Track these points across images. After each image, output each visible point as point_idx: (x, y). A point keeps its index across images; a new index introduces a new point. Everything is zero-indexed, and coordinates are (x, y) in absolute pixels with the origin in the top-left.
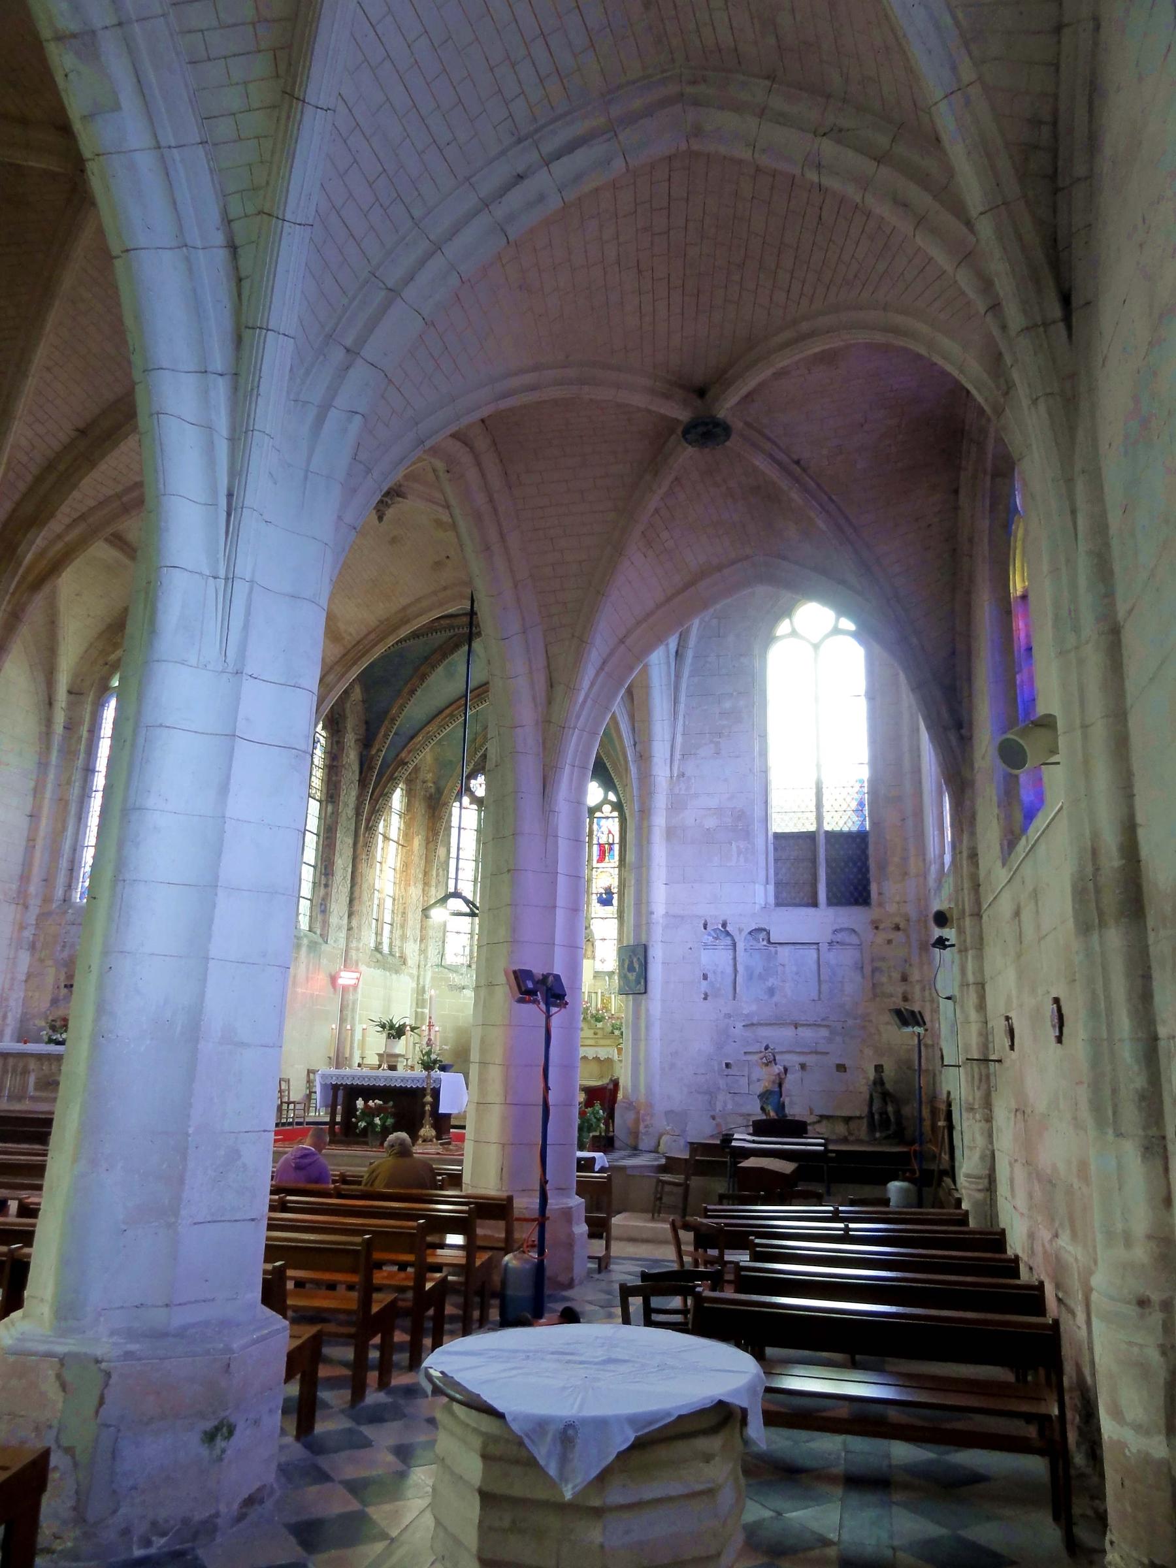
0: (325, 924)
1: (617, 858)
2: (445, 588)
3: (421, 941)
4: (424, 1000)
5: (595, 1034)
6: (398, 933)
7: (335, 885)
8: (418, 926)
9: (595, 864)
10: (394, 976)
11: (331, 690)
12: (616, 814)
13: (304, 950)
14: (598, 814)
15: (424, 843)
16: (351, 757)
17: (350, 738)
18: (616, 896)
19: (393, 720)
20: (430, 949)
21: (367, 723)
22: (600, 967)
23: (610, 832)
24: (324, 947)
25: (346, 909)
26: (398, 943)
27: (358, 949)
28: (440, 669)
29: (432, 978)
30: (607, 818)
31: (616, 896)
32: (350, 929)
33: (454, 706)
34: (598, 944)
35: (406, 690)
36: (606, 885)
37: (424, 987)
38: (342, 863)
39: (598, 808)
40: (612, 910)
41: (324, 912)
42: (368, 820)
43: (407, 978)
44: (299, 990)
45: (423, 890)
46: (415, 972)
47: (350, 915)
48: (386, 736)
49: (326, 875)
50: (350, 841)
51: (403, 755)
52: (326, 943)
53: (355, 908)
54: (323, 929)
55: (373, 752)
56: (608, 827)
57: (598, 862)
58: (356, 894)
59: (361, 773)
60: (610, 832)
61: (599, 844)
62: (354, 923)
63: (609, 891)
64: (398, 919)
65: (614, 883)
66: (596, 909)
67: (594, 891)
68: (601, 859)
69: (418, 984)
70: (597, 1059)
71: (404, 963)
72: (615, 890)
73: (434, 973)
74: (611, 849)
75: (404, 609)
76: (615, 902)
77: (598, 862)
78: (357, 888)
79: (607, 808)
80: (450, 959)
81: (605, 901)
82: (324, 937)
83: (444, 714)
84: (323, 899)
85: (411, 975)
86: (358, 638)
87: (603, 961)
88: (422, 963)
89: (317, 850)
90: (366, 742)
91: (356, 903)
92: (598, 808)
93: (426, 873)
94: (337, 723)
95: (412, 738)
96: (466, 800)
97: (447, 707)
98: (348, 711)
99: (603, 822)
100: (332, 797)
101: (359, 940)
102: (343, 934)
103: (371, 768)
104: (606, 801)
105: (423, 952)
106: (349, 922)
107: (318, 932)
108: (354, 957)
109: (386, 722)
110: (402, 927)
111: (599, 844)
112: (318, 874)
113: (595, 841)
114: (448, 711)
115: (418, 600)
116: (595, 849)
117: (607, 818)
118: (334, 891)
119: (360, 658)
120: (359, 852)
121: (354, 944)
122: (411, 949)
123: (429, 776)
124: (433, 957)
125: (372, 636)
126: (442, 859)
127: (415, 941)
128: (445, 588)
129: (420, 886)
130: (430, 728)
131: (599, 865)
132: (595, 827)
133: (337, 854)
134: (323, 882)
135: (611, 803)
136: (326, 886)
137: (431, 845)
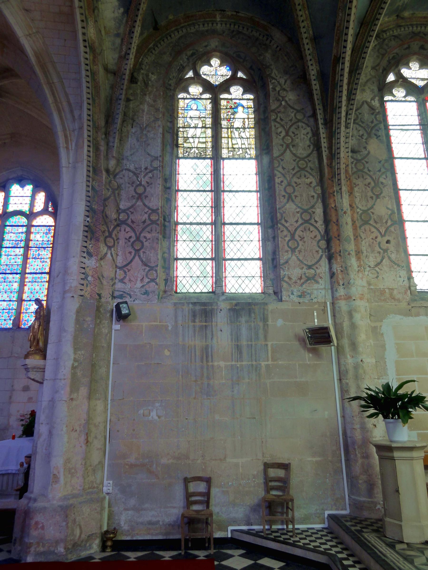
27: (348, 298)
32: (332, 275)
101: (347, 285)
121: (341, 292)
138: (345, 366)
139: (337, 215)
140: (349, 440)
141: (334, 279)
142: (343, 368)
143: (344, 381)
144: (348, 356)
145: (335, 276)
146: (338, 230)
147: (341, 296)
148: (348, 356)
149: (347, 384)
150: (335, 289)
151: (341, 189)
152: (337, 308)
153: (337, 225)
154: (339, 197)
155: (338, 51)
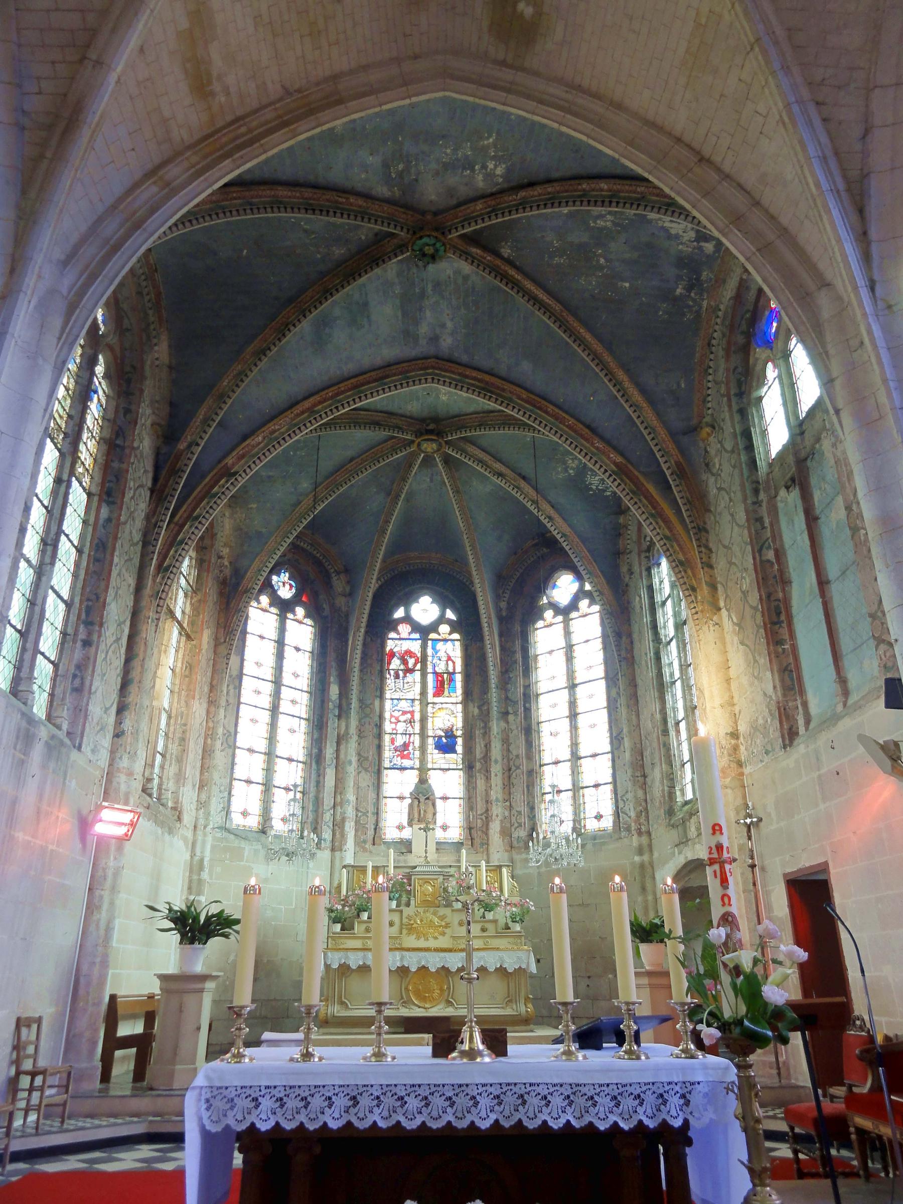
0: (80, 713)
1: (459, 691)
2: (416, 57)
3: (201, 787)
4: (200, 880)
5: (483, 930)
6: (171, 770)
7: (102, 647)
8: (199, 764)
9: (430, 698)
10: (167, 837)
11: (174, 192)
12: (456, 636)
13: (38, 751)
14: (433, 636)
15: (212, 643)
16: (144, 443)
17: (147, 415)
18: (460, 741)
19: (222, 398)
20: (214, 800)
21: (172, 404)
22: (439, 834)
23: (449, 658)
24: (74, 755)
25: (114, 696)
26: (171, 785)
27: (130, 774)
28: (305, 326)
29: (213, 847)
30: (445, 640)
31: (460, 741)
32: (118, 735)
33: (317, 398)
34: (439, 803)
35: (250, 349)
36: (448, 725)
37: (202, 861)
38: (117, 610)
39: (433, 627)
40: (456, 758)
41: (78, 690)
42: (164, 556)
43: (181, 843)
44: (20, 836)
45: (208, 712)
46: (189, 834)
47: (121, 709)
48: (207, 421)
49: (89, 623)
50: (132, 581)
51: (229, 461)
52: (79, 748)
53: (131, 699)
54: (73, 723)
55: (182, 446)
56: (449, 651)
57: (434, 696)
58: (135, 674)
59: (155, 479)
60: (449, 658)
61: (435, 673)
62: (127, 725)
63: (450, 734)
64: (174, 748)
65: (458, 722)
66: (435, 757)
67: (430, 733)
68: (439, 692)
69: (193, 855)
70: (501, 971)
71: (179, 819)
72: (459, 733)
73: (214, 839)
74: (451, 680)
75: (335, 78)
76: (459, 748)
77: (434, 696)
78: (136, 663)
79: (444, 629)
80: (237, 820)
81: (446, 746)
82: (75, 738)
83: (298, 409)
84: (78, 667)
85: (185, 839)
86: (239, 113)
87: (445, 828)
88: (202, 822)
89: (75, 576)
90: (170, 434)
91: (133, 689)
92: (433, 627)
93: (212, 688)
94: (129, 381)
95: (245, 438)
96: (264, 600)
97: (306, 398)
98: (148, 371)
99: (440, 645)
100: (109, 494)
102: (106, 742)
103: (175, 472)
104: (442, 620)
105: (202, 805)
106: (119, 722)
107: (65, 727)
108: (123, 787)
109: (209, 401)
110: (180, 761)
111: (435, 673)
112: (73, 618)
113: (430, 670)
114: (307, 404)
115: (365, 68)
116: (430, 678)
117: (445, 640)
118: (101, 656)
119: (239, 148)
120: (145, 602)
122: (188, 797)
123: (225, 551)
124: (216, 819)
125: (268, 114)
126: (235, 673)
127: (194, 786)
128: (416, 57)
129: (205, 705)
130: (272, 426)
131: (437, 700)
132: (430, 651)
133: (111, 592)
134: (82, 635)
135: (449, 622)
136: (87, 643)
137: (222, 649)
138: (104, 869)
139: (145, 651)
140: (82, 981)
141: (120, 741)
142: (100, 873)
143: (97, 893)
144: (112, 858)
145: (124, 738)
146: (142, 673)
147: (124, 768)
148: (112, 858)
149: (101, 897)
150: (118, 755)
151: (158, 619)
152: (114, 784)
153: (142, 666)
154: (153, 628)
155: (233, 465)
